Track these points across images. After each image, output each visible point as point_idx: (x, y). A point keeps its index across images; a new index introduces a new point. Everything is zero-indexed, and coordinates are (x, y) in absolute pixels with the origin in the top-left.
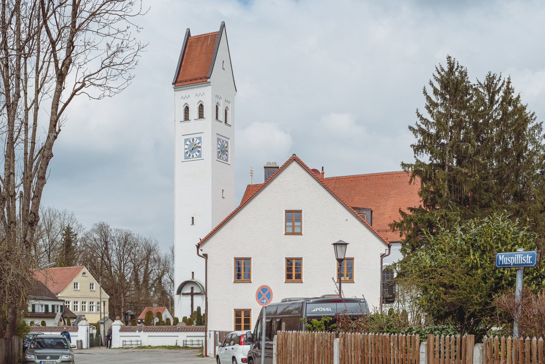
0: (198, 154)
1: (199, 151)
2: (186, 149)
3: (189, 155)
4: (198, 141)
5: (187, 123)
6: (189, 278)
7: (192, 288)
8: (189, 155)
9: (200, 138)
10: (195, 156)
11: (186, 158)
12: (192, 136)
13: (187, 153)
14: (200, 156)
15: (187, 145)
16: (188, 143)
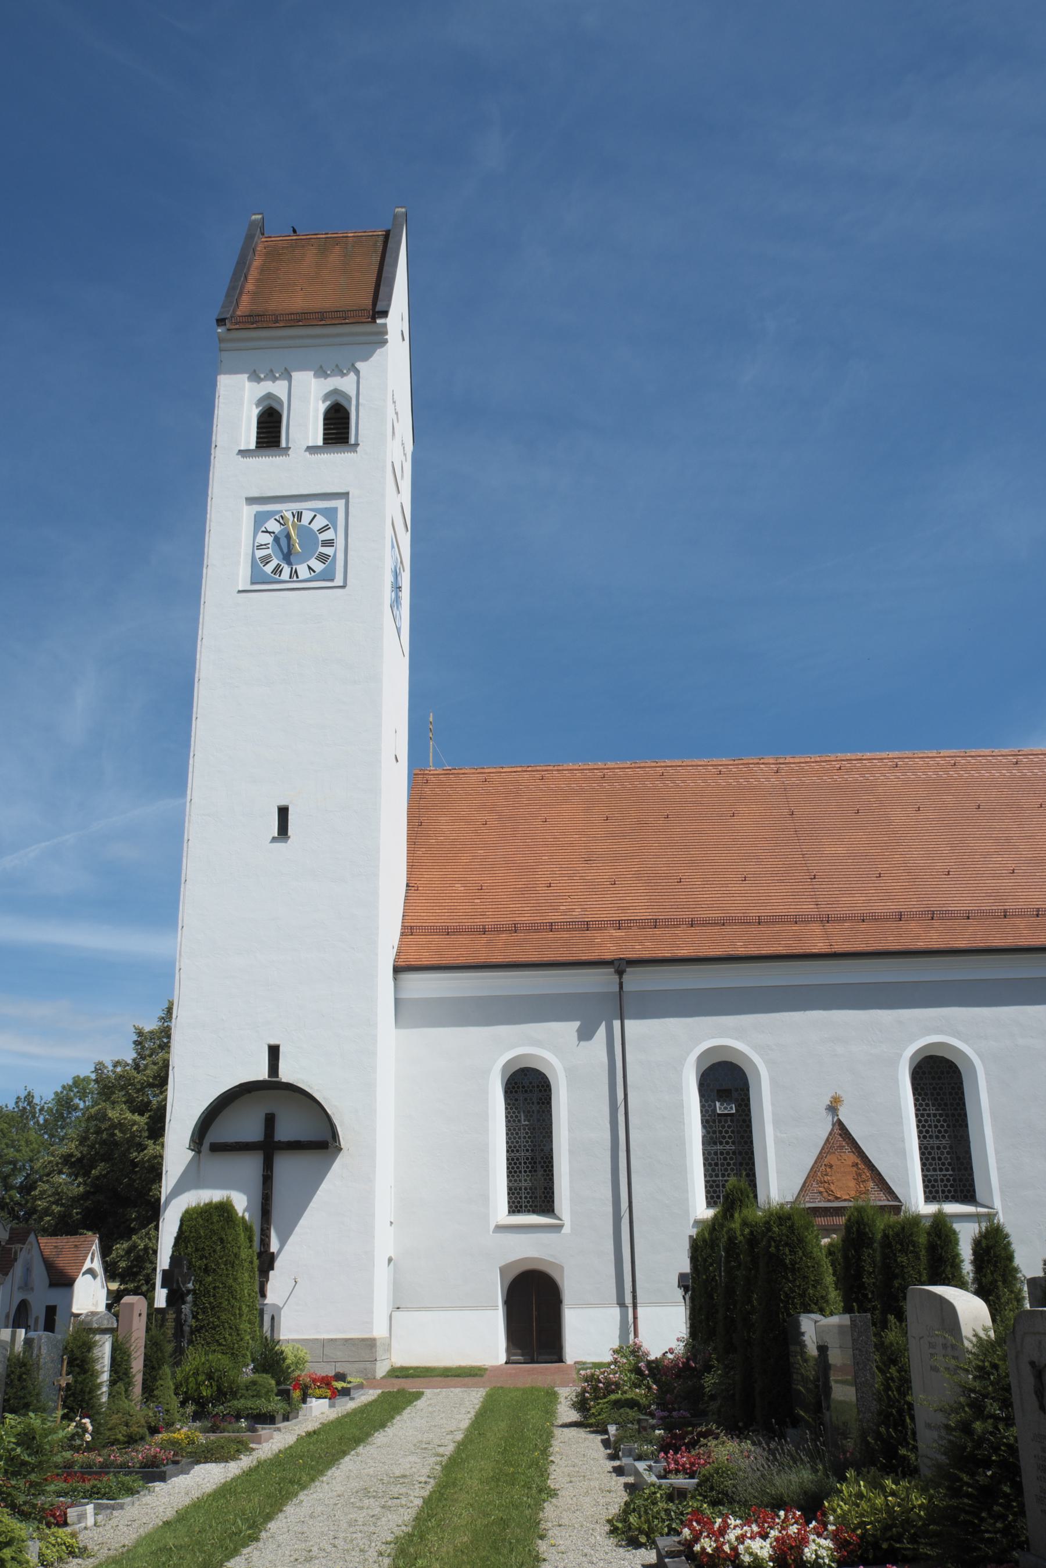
0: (318, 566)
1: (323, 558)
2: (260, 547)
3: (278, 570)
4: (320, 521)
5: (268, 462)
6: (262, 1073)
7: (270, 1121)
8: (278, 570)
9: (330, 514)
10: (303, 571)
11: (258, 578)
12: (296, 506)
13: (266, 560)
14: (328, 575)
15: (267, 532)
16: (273, 525)
